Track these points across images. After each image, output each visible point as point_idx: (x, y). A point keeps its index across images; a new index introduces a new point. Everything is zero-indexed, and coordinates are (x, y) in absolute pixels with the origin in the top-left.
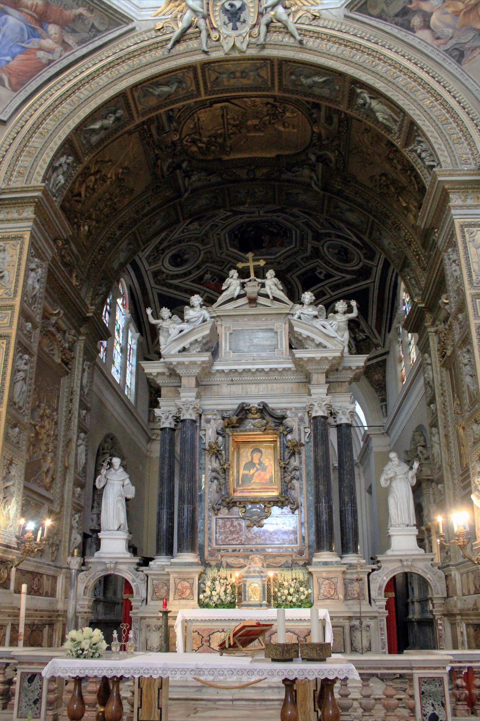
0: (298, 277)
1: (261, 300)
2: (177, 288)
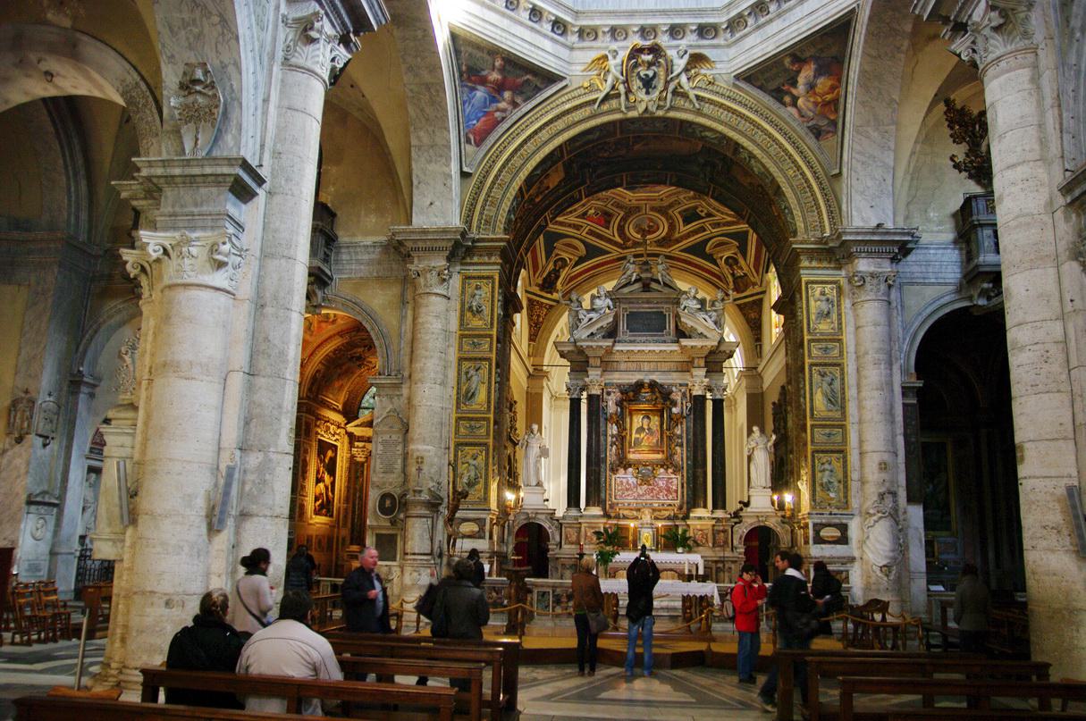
0: (680, 213)
1: (654, 285)
2: (561, 224)
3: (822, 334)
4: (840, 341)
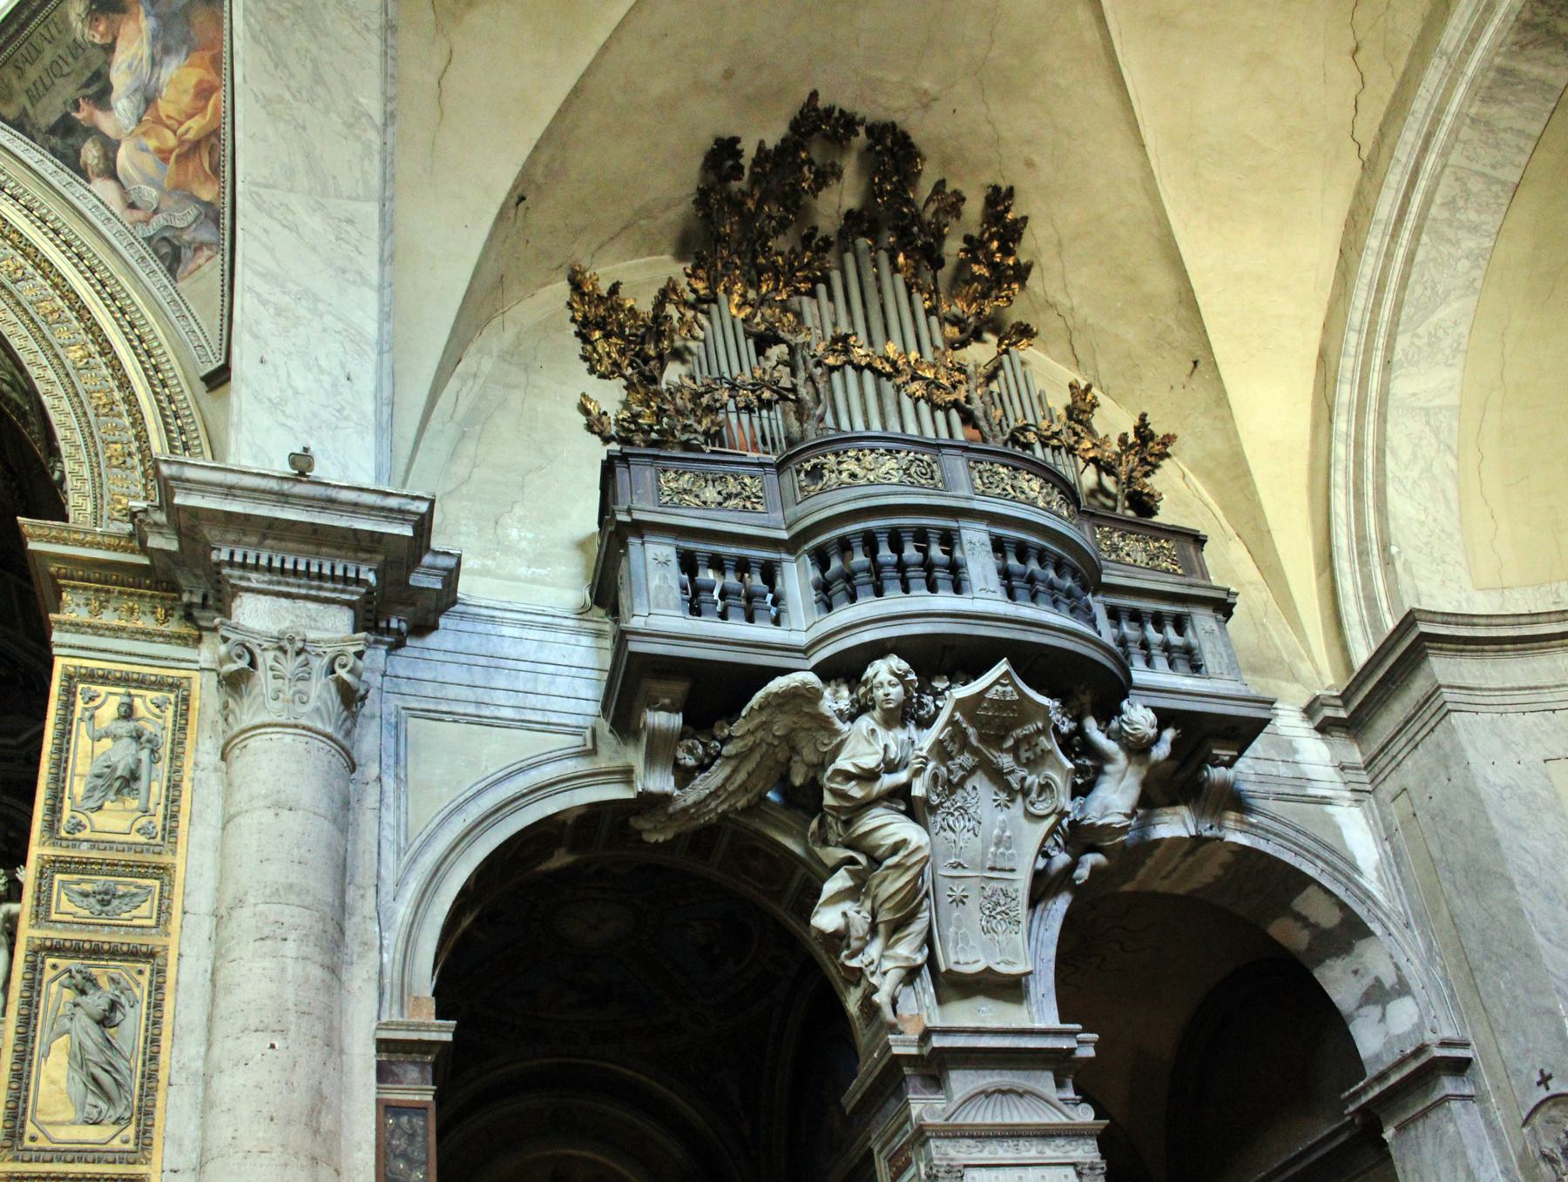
3: (94, 844)
4: (162, 872)
